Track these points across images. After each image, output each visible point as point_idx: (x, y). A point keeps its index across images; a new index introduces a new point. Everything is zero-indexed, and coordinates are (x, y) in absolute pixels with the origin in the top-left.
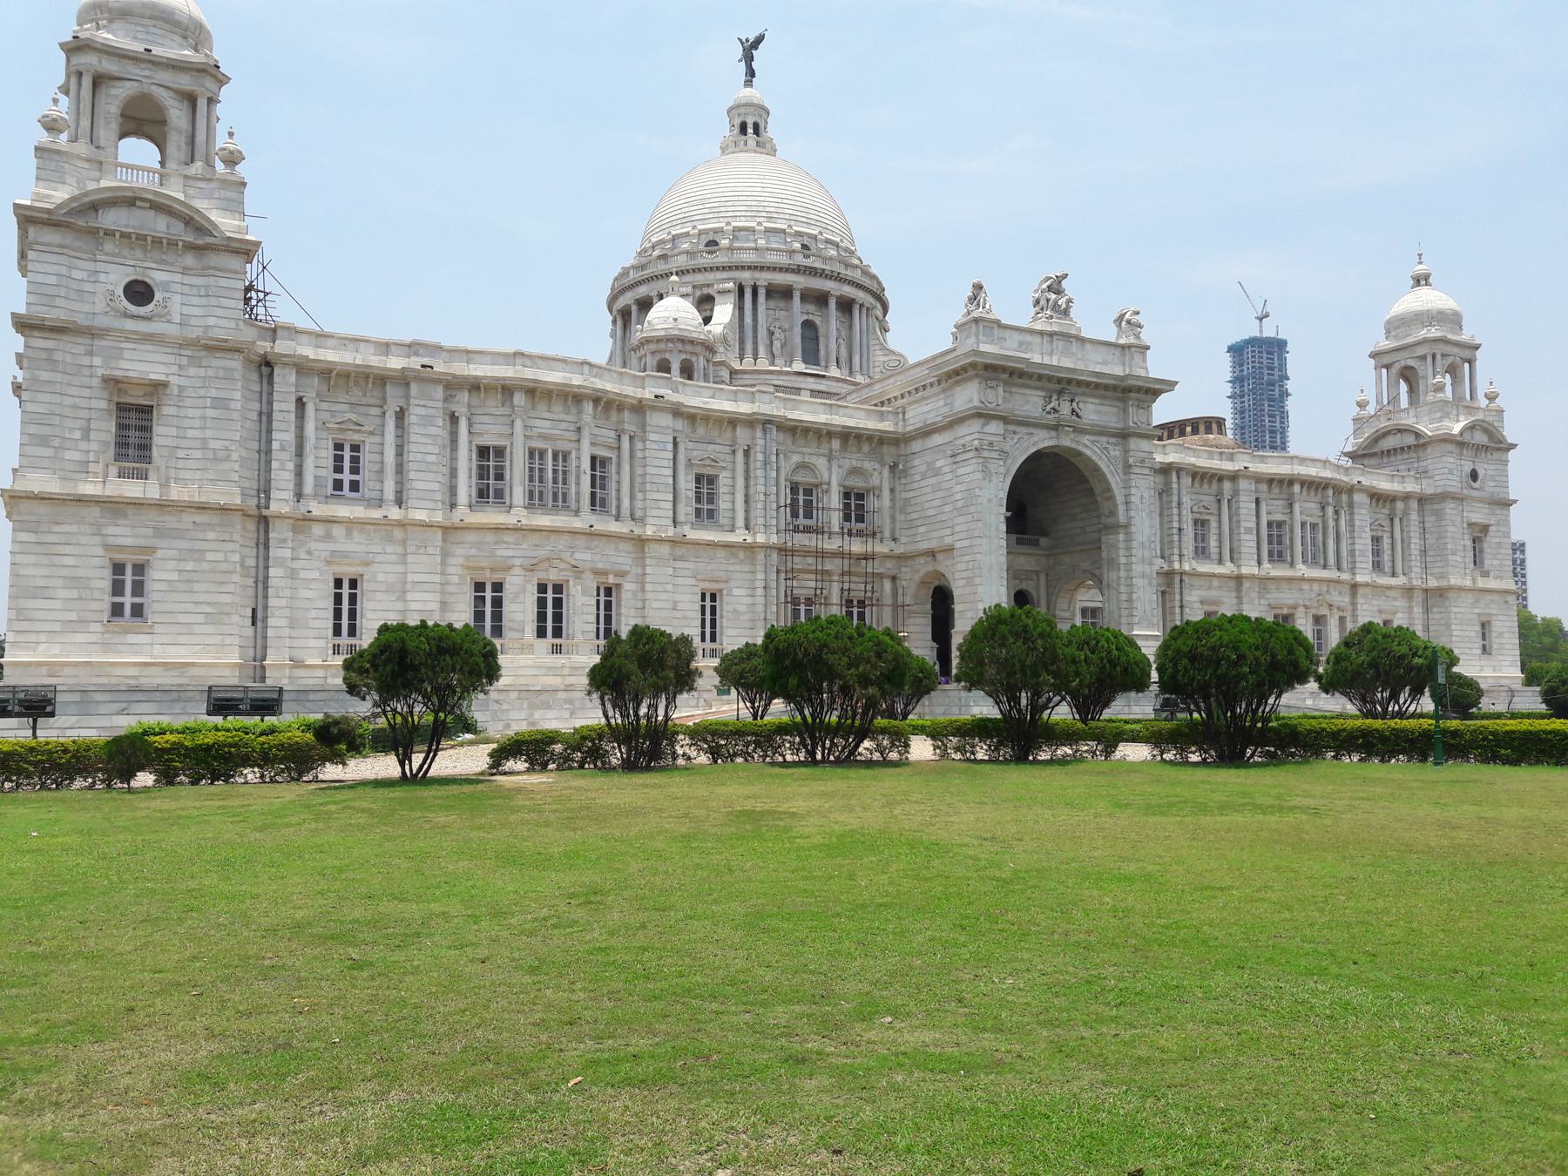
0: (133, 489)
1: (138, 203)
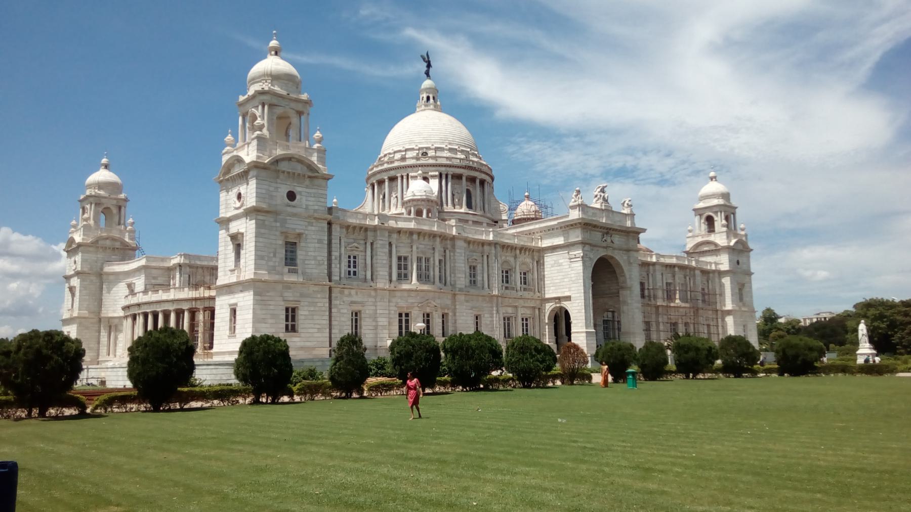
1: (293, 160)
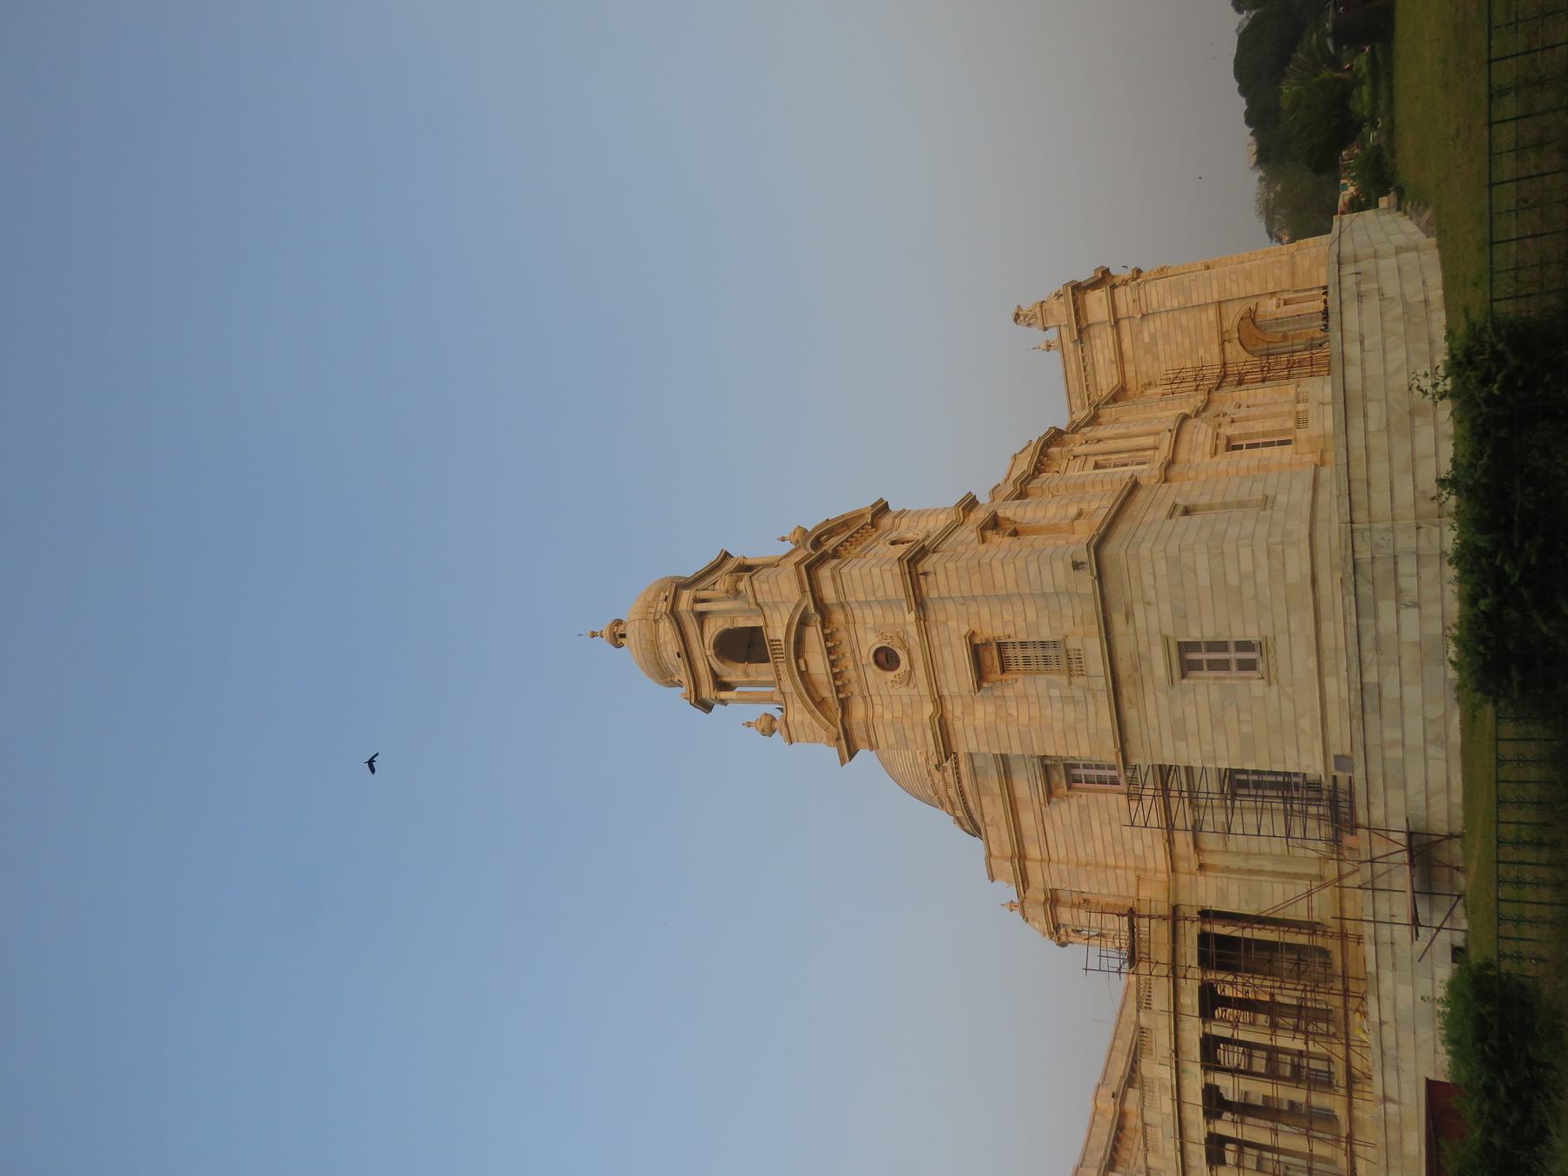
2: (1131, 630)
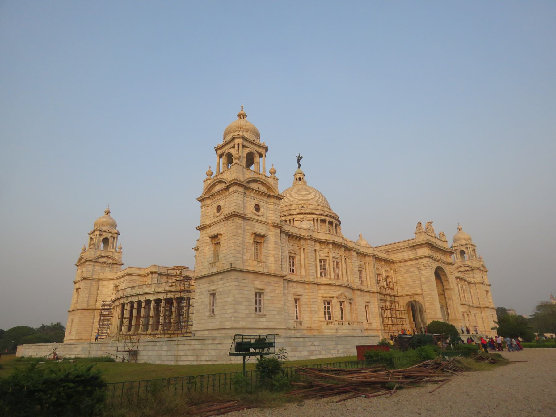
0: (260, 269)
1: (259, 182)
2: (219, 280)
